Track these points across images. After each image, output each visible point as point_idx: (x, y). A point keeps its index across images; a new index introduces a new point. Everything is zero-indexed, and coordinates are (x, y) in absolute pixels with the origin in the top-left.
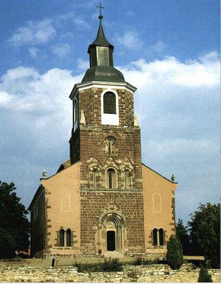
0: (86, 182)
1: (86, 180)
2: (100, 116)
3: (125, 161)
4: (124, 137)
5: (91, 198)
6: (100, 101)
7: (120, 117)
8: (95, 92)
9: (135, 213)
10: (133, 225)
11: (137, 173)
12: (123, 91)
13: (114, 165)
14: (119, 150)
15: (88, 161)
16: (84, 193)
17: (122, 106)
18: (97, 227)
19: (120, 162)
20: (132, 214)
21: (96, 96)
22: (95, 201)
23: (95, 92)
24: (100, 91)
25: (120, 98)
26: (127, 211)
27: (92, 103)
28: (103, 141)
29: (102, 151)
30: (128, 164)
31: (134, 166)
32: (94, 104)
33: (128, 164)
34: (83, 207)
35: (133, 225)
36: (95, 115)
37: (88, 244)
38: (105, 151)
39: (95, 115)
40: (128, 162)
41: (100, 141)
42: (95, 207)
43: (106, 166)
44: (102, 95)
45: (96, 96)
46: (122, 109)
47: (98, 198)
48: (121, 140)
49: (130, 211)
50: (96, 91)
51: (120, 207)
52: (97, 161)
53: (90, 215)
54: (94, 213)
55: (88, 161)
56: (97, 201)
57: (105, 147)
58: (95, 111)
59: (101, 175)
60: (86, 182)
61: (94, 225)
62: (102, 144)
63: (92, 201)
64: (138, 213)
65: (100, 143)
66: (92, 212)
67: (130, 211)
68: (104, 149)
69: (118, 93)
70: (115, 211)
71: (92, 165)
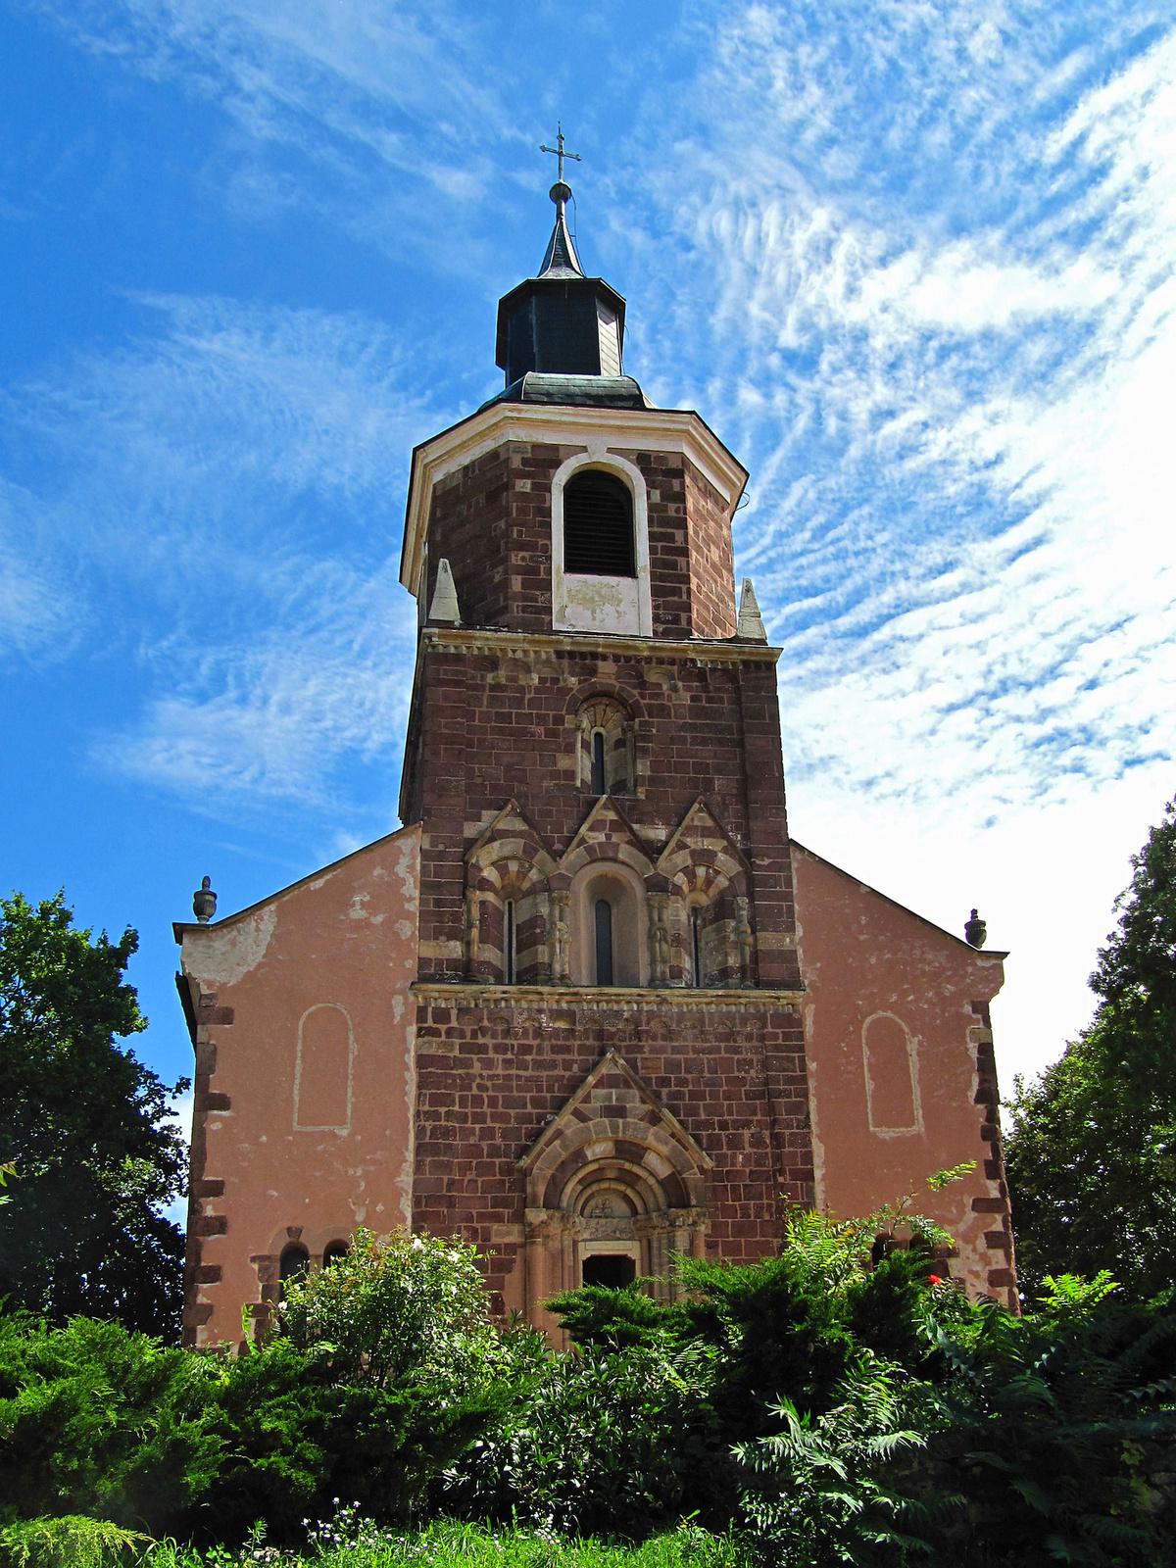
0: (455, 949)
1: (452, 935)
2: (547, 586)
3: (691, 830)
4: (685, 698)
5: (483, 1049)
6: (547, 513)
7: (656, 592)
8: (516, 462)
9: (757, 1141)
10: (745, 1214)
11: (766, 896)
12: (675, 464)
13: (625, 852)
14: (655, 766)
15: (470, 830)
16: (442, 1015)
17: (671, 538)
18: (516, 1228)
19: (659, 833)
20: (735, 1143)
21: (524, 486)
22: (507, 1063)
23: (516, 462)
24: (546, 459)
25: (656, 496)
26: (709, 1125)
27: (502, 524)
28: (559, 720)
29: (555, 775)
30: (707, 844)
31: (746, 857)
32: (509, 526)
33: (707, 844)
34: (436, 1100)
35: (745, 1214)
36: (517, 583)
38: (570, 775)
39: (517, 583)
40: (705, 832)
41: (541, 719)
42: (509, 1103)
43: (574, 855)
44: (561, 477)
45: (524, 486)
46: (667, 550)
47: (526, 1049)
48: (663, 711)
49: (723, 1126)
50: (525, 462)
51: (665, 1099)
52: (520, 825)
53: (474, 1151)
54: (498, 1141)
55: (470, 830)
56: (524, 1066)
57: (570, 749)
58: (517, 558)
59: (544, 910)
60: (455, 949)
61: (498, 1218)
62: (552, 734)
63: (488, 1064)
64: (777, 1138)
65: (540, 730)
66: (487, 1133)
67: (723, 1126)
68: (563, 763)
69: (644, 471)
70: (633, 1127)
71: (496, 849)
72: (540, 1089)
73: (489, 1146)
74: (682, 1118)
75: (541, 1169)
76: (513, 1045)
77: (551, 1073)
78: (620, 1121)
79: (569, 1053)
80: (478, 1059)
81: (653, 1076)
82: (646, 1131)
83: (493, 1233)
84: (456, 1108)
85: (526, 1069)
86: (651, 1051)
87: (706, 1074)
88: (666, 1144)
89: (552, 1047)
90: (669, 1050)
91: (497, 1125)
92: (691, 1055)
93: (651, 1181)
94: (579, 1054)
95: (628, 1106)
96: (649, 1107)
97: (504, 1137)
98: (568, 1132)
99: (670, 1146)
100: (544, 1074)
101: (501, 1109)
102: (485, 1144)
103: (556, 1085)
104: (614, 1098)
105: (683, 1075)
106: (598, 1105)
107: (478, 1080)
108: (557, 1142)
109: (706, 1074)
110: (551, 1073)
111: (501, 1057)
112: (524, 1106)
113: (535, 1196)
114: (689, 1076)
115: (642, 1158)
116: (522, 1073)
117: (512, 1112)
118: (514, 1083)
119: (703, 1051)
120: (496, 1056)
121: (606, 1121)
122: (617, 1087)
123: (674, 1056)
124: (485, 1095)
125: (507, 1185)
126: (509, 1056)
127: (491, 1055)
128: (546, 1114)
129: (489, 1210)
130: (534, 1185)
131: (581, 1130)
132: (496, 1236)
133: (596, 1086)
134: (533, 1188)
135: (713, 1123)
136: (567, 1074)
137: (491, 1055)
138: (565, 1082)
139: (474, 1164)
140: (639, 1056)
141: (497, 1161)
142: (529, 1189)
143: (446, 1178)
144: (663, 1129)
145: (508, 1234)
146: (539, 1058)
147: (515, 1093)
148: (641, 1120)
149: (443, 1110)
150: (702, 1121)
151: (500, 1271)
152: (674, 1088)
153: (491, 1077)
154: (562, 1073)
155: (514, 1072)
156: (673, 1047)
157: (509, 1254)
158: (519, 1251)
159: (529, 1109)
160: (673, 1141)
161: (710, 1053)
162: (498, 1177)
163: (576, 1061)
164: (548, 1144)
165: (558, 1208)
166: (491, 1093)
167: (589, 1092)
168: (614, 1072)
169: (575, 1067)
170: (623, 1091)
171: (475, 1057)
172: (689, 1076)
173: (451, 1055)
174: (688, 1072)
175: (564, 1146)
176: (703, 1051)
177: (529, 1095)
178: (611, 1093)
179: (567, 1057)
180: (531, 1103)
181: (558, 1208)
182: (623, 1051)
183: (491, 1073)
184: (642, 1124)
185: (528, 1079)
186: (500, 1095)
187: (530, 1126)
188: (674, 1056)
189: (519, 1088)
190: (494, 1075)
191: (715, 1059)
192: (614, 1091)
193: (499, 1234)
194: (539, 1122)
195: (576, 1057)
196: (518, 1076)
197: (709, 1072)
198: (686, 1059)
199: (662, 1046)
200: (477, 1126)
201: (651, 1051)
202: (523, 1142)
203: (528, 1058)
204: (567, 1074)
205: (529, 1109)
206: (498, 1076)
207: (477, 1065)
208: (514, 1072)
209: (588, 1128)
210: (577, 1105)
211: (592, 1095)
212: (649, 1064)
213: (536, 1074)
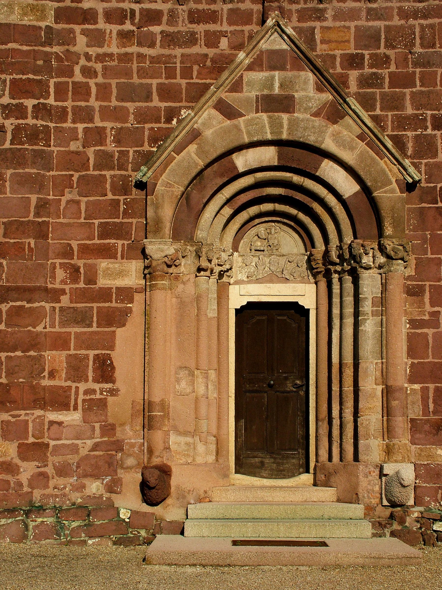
37: (53, 416)
72: (171, 74)
73: (97, 153)
74: (378, 112)
75: (168, 185)
76: (133, 12)
77: (187, 51)
78: (285, 117)
79: (215, 22)
80: (84, 32)
81: (338, 53)
82: (322, 132)
83: (100, 272)
84: (51, 101)
85: (152, 45)
86: (335, 18)
87: (418, 49)
88: (352, 149)
89: (191, 13)
90: (364, 14)
91: (108, 125)
92: (397, 21)
93: (331, 200)
94: (230, 24)
95: (296, 95)
96: (327, 97)
97: (118, 141)
98: (208, 133)
99: (357, 152)
100: (178, 52)
101: (114, 103)
102: (91, 152)
103: (196, 68)
104: (277, 85)
105: (382, 50)
106: (253, 94)
107: (83, 61)
108: (192, 148)
109: (418, 49)
110: (187, 51)
111: (115, 28)
112: (148, 98)
113: (158, 222)
114: (391, 53)
115: (317, 169)
116: (145, 51)
117: (131, 106)
118: (135, 66)
119: (415, 14)
120: (108, 27)
121: (264, 116)
122: (282, 68)
123: (371, 24)
124: (92, 82)
125: (122, 207)
126: (128, 26)
127: (101, 24)
128: (180, 108)
129: (96, 241)
130: (157, 207)
131: (226, 131)
132: (104, 277)
133: (250, 68)
134: (155, 212)
135: (425, 119)
136: (211, 52)
137: (101, 24)
138: (209, 63)
139: (75, 179)
140: (317, 24)
141: (108, 174)
142: (150, 213)
143: (34, 198)
144: (348, 128)
145: (121, 274)
146: (171, 29)
147: (136, 80)
148: (316, 114)
149: (30, 103)
150: (408, 118)
151: (110, 324)
152: (367, 70)
153: (100, 58)
154: (205, 50)
155: (134, 49)
156: (369, 11)
157: (122, 301)
158: (139, 298)
159: (156, 102)
160: (362, 145)
161: (425, 17)
162: (110, 196)
163: (224, 34)
164: (179, 150)
165: (190, 239)
166: (100, 79)
167: (241, 76)
168: (277, 47)
169: (224, 43)
170: (289, 74)
171: (77, 28)
172: (391, 53)
173: (43, 24)
174: (390, 45)
175: (200, 152)
176: (415, 14)
177: (155, 82)
178: (273, 77)
179: (212, 27)
180: (159, 95)
181: (190, 239)
182: (295, 17)
183: (100, 51)
184: (318, 122)
185: (154, 60)
186: (113, 82)
187: (156, 126)
188: (371, 24)
189: (142, 73)
190: (106, 55)
191: (432, 26)
192: (277, 73)
193: (108, 274)
194: (169, 120)
195: (225, 27)
196: (141, 56)
197: (422, 46)
198: (388, 28)
199: (352, 10)
200: (81, 127)
201: (335, 18)
202: (146, 147)
203: (156, 29)
204: (211, 52)
205: (156, 102)
206: (111, 55)
207: (81, 40)
208: (134, 49)
209: (237, 127)
210: (223, 95)
211: (245, 79)
212: (333, 36)
213: (166, 52)
